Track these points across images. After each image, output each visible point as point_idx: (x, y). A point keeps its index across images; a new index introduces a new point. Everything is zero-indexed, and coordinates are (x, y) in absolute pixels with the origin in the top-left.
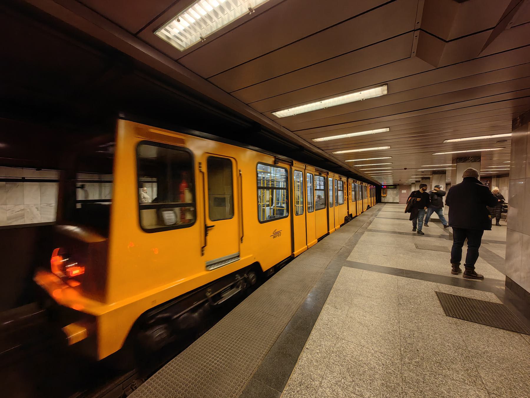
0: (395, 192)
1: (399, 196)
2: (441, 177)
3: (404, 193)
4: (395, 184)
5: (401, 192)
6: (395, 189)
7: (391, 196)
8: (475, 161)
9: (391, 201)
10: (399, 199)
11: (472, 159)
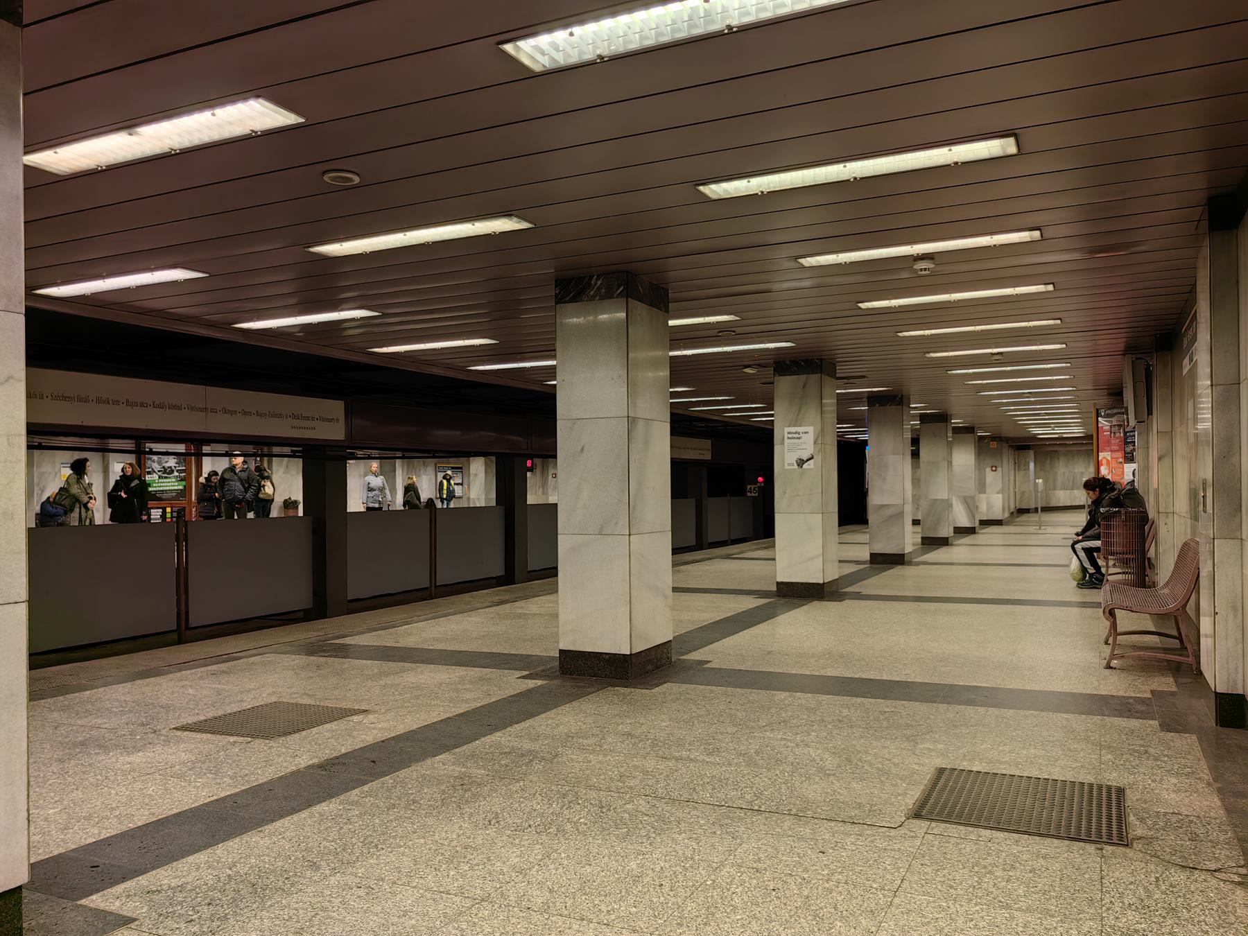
2: (804, 386)
11: (599, 282)
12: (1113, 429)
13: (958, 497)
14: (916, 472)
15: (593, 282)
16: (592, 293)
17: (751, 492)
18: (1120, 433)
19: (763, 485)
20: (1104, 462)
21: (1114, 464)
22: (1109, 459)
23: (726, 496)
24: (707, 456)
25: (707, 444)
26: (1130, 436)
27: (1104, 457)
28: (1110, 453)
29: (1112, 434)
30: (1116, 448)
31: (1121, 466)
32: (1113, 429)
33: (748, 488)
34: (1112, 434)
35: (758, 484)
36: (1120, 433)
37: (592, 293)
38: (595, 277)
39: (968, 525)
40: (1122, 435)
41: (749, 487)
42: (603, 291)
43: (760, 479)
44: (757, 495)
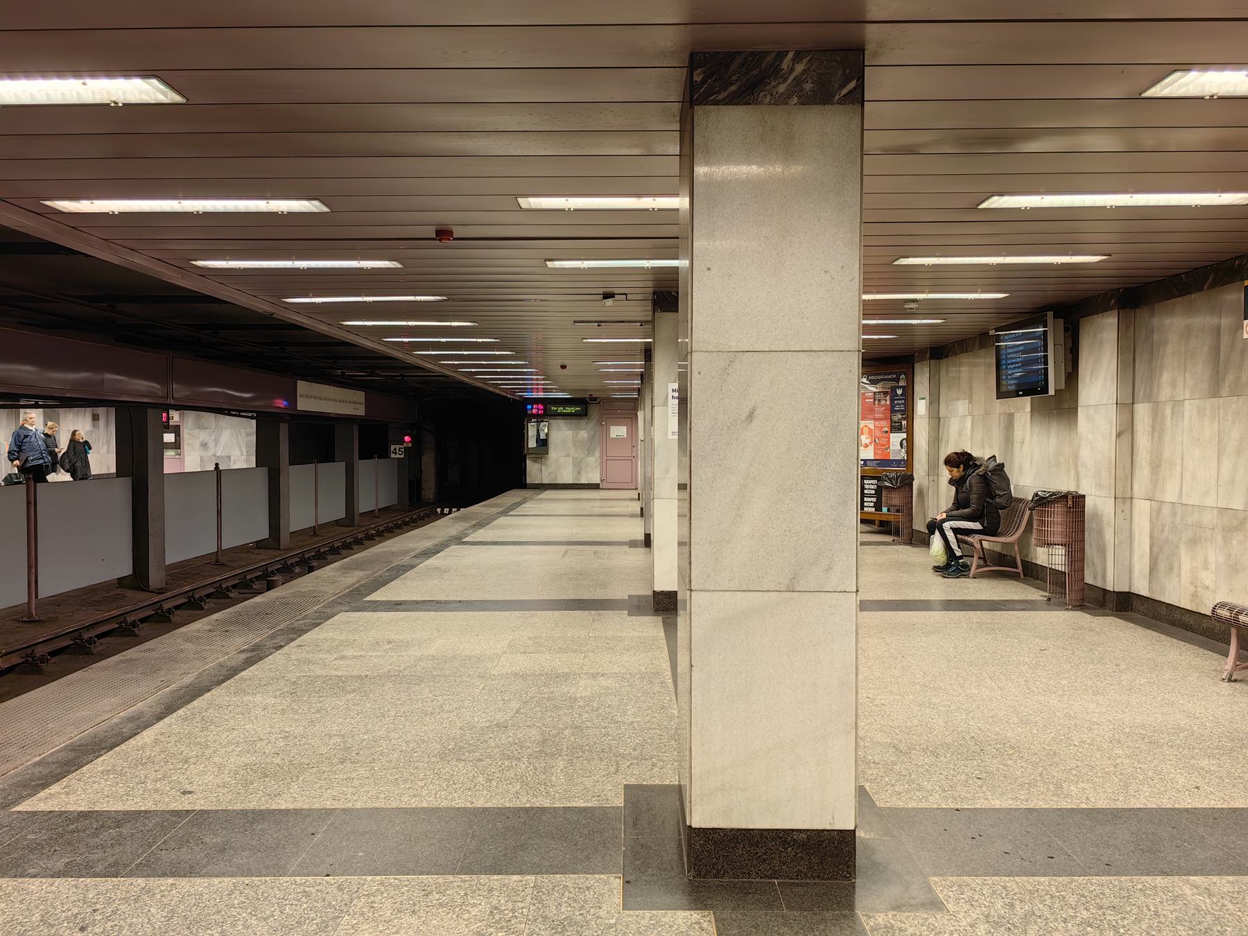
0: (583, 434)
1: (601, 458)
3: (618, 440)
4: (579, 396)
6: (583, 422)
7: (568, 456)
8: (821, 96)
9: (567, 478)
10: (601, 464)
11: (799, 68)
12: (877, 396)
14: (578, 433)
15: (785, 65)
16: (782, 88)
17: (396, 453)
18: (886, 400)
19: (410, 445)
20: (866, 430)
21: (878, 433)
22: (872, 427)
23: (372, 458)
24: (360, 411)
25: (360, 396)
26: (897, 404)
27: (866, 426)
28: (873, 421)
29: (877, 402)
30: (881, 416)
31: (886, 435)
32: (877, 396)
34: (877, 402)
35: (405, 445)
36: (886, 400)
37: (782, 88)
38: (791, 55)
40: (888, 403)
41: (393, 447)
42: (808, 86)
43: (407, 438)
44: (402, 456)
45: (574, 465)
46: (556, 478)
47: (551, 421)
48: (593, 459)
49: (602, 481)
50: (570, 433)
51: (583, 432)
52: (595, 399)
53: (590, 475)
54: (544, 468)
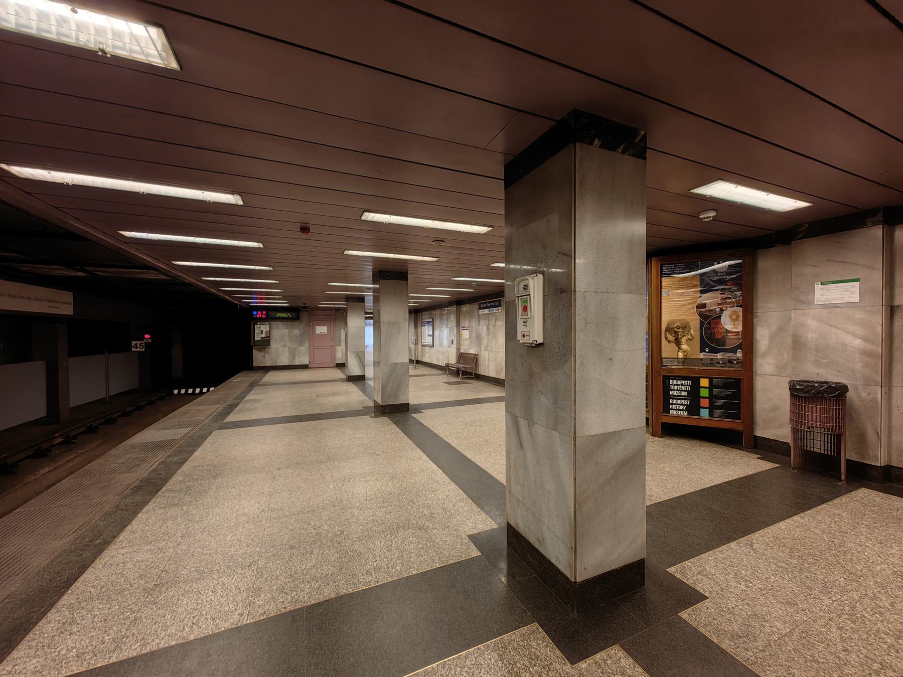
0: (296, 332)
3: (321, 335)
5: (314, 330)
6: (296, 323)
7: (285, 346)
9: (284, 360)
13: (353, 352)
14: (292, 331)
17: (137, 347)
19: (150, 341)
33: (133, 345)
35: (145, 341)
39: (360, 374)
41: (134, 343)
44: (143, 350)
45: (290, 353)
46: (276, 362)
47: (272, 323)
48: (304, 349)
49: (310, 363)
50: (287, 330)
51: (296, 330)
52: (306, 307)
53: (302, 359)
54: (266, 355)
